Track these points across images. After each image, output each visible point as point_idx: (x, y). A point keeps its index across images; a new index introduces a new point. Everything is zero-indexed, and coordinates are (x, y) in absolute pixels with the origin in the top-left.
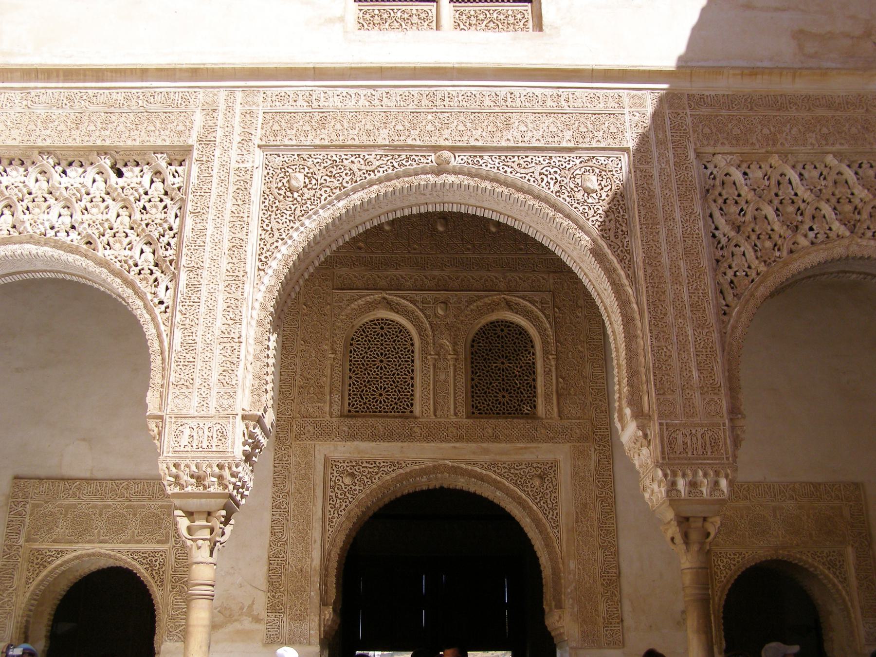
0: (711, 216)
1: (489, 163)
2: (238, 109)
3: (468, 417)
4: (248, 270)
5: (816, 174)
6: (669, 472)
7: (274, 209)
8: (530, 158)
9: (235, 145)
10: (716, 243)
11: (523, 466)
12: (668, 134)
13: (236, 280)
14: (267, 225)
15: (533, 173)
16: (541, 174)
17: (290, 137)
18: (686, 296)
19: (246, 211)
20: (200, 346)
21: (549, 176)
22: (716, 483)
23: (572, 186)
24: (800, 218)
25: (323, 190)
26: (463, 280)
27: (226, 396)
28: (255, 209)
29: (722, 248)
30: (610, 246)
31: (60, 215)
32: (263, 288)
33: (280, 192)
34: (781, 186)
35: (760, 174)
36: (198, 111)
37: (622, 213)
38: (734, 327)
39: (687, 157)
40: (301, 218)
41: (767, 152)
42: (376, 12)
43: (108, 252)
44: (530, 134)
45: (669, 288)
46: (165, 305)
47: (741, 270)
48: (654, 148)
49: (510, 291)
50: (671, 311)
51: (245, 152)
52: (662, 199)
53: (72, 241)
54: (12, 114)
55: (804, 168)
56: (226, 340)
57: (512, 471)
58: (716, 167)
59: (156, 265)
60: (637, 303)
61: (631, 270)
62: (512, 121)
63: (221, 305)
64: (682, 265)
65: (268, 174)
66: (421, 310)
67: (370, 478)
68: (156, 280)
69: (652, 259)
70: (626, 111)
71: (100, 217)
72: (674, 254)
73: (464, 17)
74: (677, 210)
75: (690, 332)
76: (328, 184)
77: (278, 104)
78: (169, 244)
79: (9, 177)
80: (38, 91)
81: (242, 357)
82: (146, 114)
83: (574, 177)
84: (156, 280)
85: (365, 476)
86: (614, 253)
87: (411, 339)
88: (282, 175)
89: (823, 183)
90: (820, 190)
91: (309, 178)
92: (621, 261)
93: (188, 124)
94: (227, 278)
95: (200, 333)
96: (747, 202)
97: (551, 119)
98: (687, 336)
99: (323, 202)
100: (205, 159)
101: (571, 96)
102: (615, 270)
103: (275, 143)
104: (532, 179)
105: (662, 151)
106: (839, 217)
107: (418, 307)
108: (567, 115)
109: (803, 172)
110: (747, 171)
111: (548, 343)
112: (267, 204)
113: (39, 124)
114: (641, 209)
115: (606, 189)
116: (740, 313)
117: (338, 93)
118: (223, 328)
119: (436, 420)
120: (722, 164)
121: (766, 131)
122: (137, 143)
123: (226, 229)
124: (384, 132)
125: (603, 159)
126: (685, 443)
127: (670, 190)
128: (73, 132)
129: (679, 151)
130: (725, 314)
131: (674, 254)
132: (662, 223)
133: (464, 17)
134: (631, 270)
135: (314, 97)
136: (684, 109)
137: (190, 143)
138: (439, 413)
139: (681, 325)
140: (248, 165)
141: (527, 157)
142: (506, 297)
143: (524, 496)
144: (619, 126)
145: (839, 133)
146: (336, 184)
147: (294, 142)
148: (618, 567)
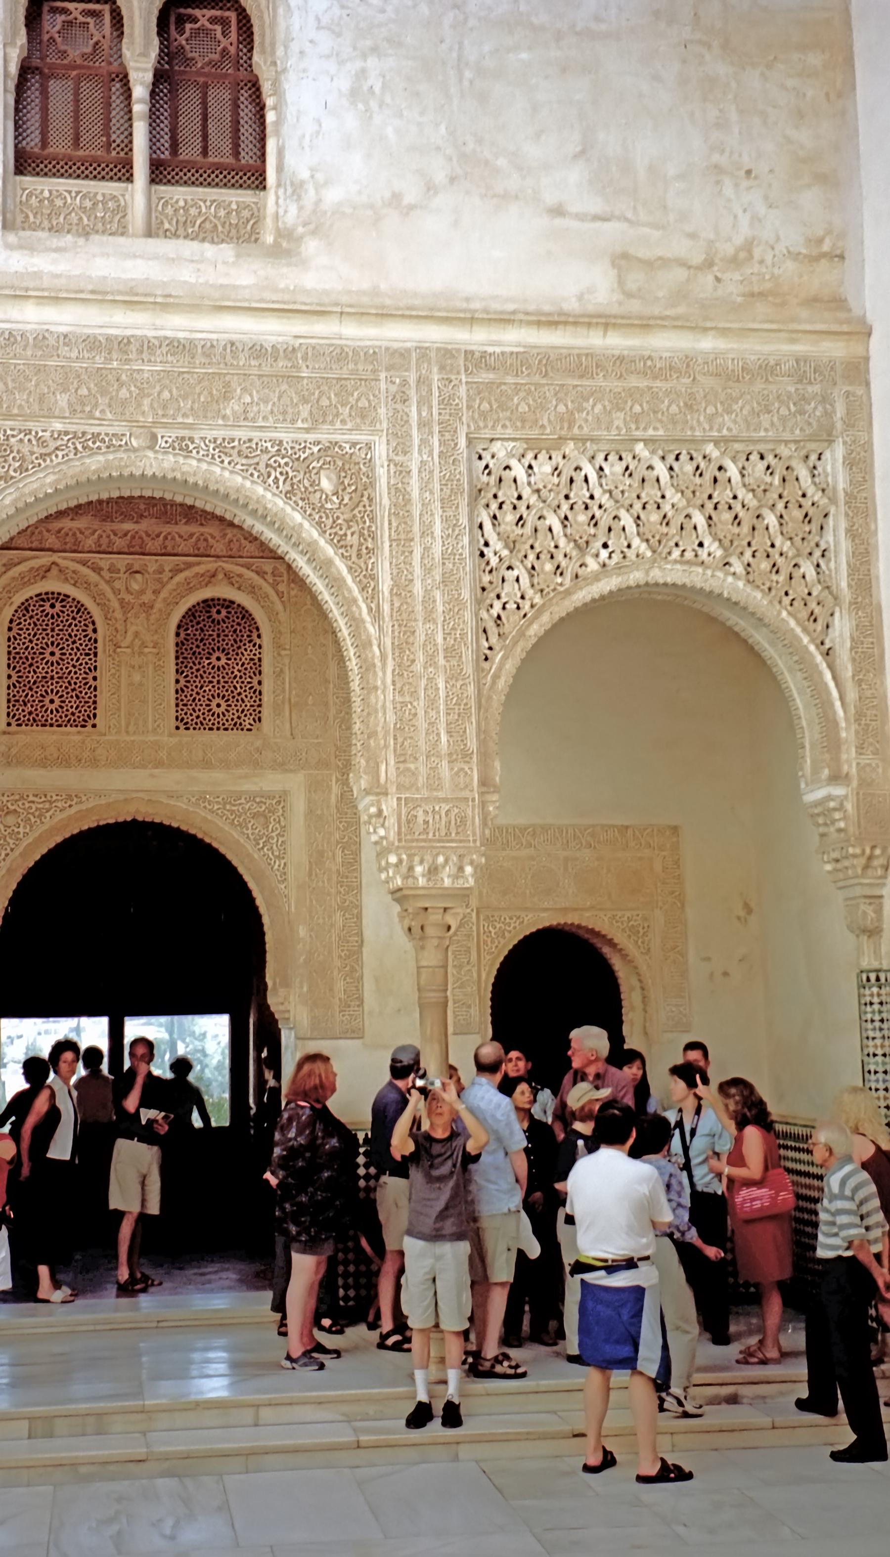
0: (481, 526)
3: (171, 735)
5: (619, 468)
6: (404, 857)
8: (254, 442)
10: (484, 565)
11: (243, 801)
12: (435, 411)
15: (258, 464)
16: (267, 466)
18: (440, 639)
21: (279, 470)
22: (461, 869)
24: (592, 531)
26: (166, 538)
29: (491, 571)
30: (350, 569)
34: (574, 484)
35: (548, 469)
37: (368, 524)
38: (496, 677)
39: (456, 444)
44: (255, 409)
45: (421, 629)
47: (512, 602)
48: (415, 432)
49: (230, 557)
50: (421, 657)
52: (419, 506)
55: (606, 459)
57: (228, 807)
58: (493, 457)
60: (379, 646)
61: (375, 601)
66: (108, 582)
67: (40, 816)
69: (401, 588)
70: (382, 376)
75: (441, 685)
83: (310, 472)
85: (33, 814)
86: (354, 579)
87: (93, 623)
89: (628, 481)
92: (363, 589)
96: (528, 507)
97: (284, 387)
98: (437, 689)
102: (355, 601)
104: (256, 474)
105: (425, 436)
107: (102, 577)
109: (604, 465)
111: (280, 632)
114: (393, 518)
115: (349, 490)
116: (505, 658)
119: (128, 738)
120: (501, 454)
121: (561, 408)
126: (426, 822)
127: (432, 493)
129: (447, 436)
130: (486, 659)
131: (429, 581)
132: (417, 539)
134: (375, 601)
136: (458, 373)
138: (132, 728)
139: (431, 676)
142: (224, 565)
143: (242, 841)
144: (371, 398)
145: (655, 412)
148: (360, 934)
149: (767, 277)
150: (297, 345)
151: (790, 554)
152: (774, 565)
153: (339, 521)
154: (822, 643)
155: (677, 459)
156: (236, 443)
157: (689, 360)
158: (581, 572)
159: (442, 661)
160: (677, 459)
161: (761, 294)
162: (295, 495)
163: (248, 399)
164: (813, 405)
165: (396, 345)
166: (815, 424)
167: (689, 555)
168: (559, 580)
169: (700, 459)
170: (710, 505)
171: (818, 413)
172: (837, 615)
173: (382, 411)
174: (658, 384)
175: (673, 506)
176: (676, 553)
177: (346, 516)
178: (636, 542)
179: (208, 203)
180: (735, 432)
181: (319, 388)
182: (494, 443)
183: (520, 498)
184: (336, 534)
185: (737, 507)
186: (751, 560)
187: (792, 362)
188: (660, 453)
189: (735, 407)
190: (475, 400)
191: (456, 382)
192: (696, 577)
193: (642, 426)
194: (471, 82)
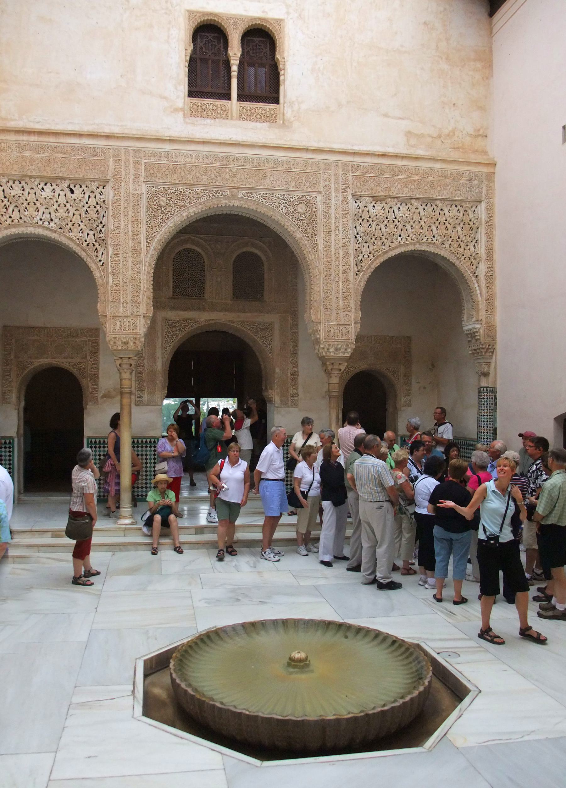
0: (356, 227)
1: (255, 196)
2: (132, 160)
4: (142, 247)
7: (153, 216)
9: (131, 180)
12: (340, 185)
13: (136, 251)
14: (150, 224)
17: (159, 177)
18: (340, 267)
19: (139, 216)
20: (121, 283)
23: (293, 210)
24: (396, 230)
25: (176, 207)
27: (135, 308)
28: (143, 215)
29: (359, 244)
31: (44, 213)
32: (149, 256)
33: (155, 207)
36: (111, 160)
40: (166, 221)
41: (385, 196)
42: (199, 104)
43: (71, 234)
44: (275, 182)
45: (334, 264)
46: (102, 262)
48: (333, 192)
50: (334, 274)
51: (137, 185)
52: (334, 219)
53: (52, 227)
54: (12, 156)
56: (133, 281)
59: (96, 241)
62: (267, 174)
63: (130, 264)
64: (340, 252)
65: (149, 197)
68: (96, 249)
70: (321, 172)
71: (64, 214)
72: (337, 246)
73: (244, 110)
74: (340, 224)
75: (341, 284)
76: (178, 204)
77: (152, 158)
78: (101, 231)
79: (14, 190)
80: (25, 142)
81: (142, 289)
82: (83, 159)
84: (96, 249)
88: (156, 198)
89: (409, 213)
90: (407, 217)
91: (169, 200)
93: (106, 167)
94: (132, 251)
95: (121, 277)
99: (176, 214)
100: (116, 187)
101: (295, 162)
103: (151, 181)
104: (275, 206)
106: (413, 230)
108: (293, 173)
109: (400, 207)
110: (375, 205)
112: (149, 213)
113: (28, 162)
117: (182, 154)
118: (132, 275)
122: (81, 177)
123: (130, 226)
124: (205, 178)
125: (308, 197)
127: (339, 214)
128: (46, 168)
130: (357, 275)
133: (244, 110)
135: (170, 155)
137: (108, 178)
140: (139, 192)
141: (273, 194)
146: (182, 204)
147: (161, 181)
149: (460, 142)
150: (290, 160)
151: (465, 242)
152: (459, 245)
153: (305, 224)
154: (475, 273)
155: (426, 206)
156: (268, 195)
157: (432, 169)
158: (391, 245)
159: (341, 275)
160: (426, 206)
161: (458, 148)
162: (289, 214)
163: (272, 179)
164: (475, 189)
165: (326, 161)
166: (475, 195)
167: (430, 240)
168: (383, 247)
169: (434, 206)
170: (437, 223)
171: (476, 192)
172: (480, 263)
173: (321, 185)
174: (420, 178)
175: (424, 222)
176: (425, 240)
177: (308, 222)
178: (411, 235)
179: (258, 108)
180: (447, 197)
181: (298, 175)
182: (361, 197)
183: (370, 217)
184: (303, 228)
185: (447, 223)
186: (451, 243)
187: (468, 173)
188: (421, 203)
189: (447, 188)
190: (354, 182)
191: (348, 175)
192: (432, 249)
193: (414, 193)
194: (355, 67)
